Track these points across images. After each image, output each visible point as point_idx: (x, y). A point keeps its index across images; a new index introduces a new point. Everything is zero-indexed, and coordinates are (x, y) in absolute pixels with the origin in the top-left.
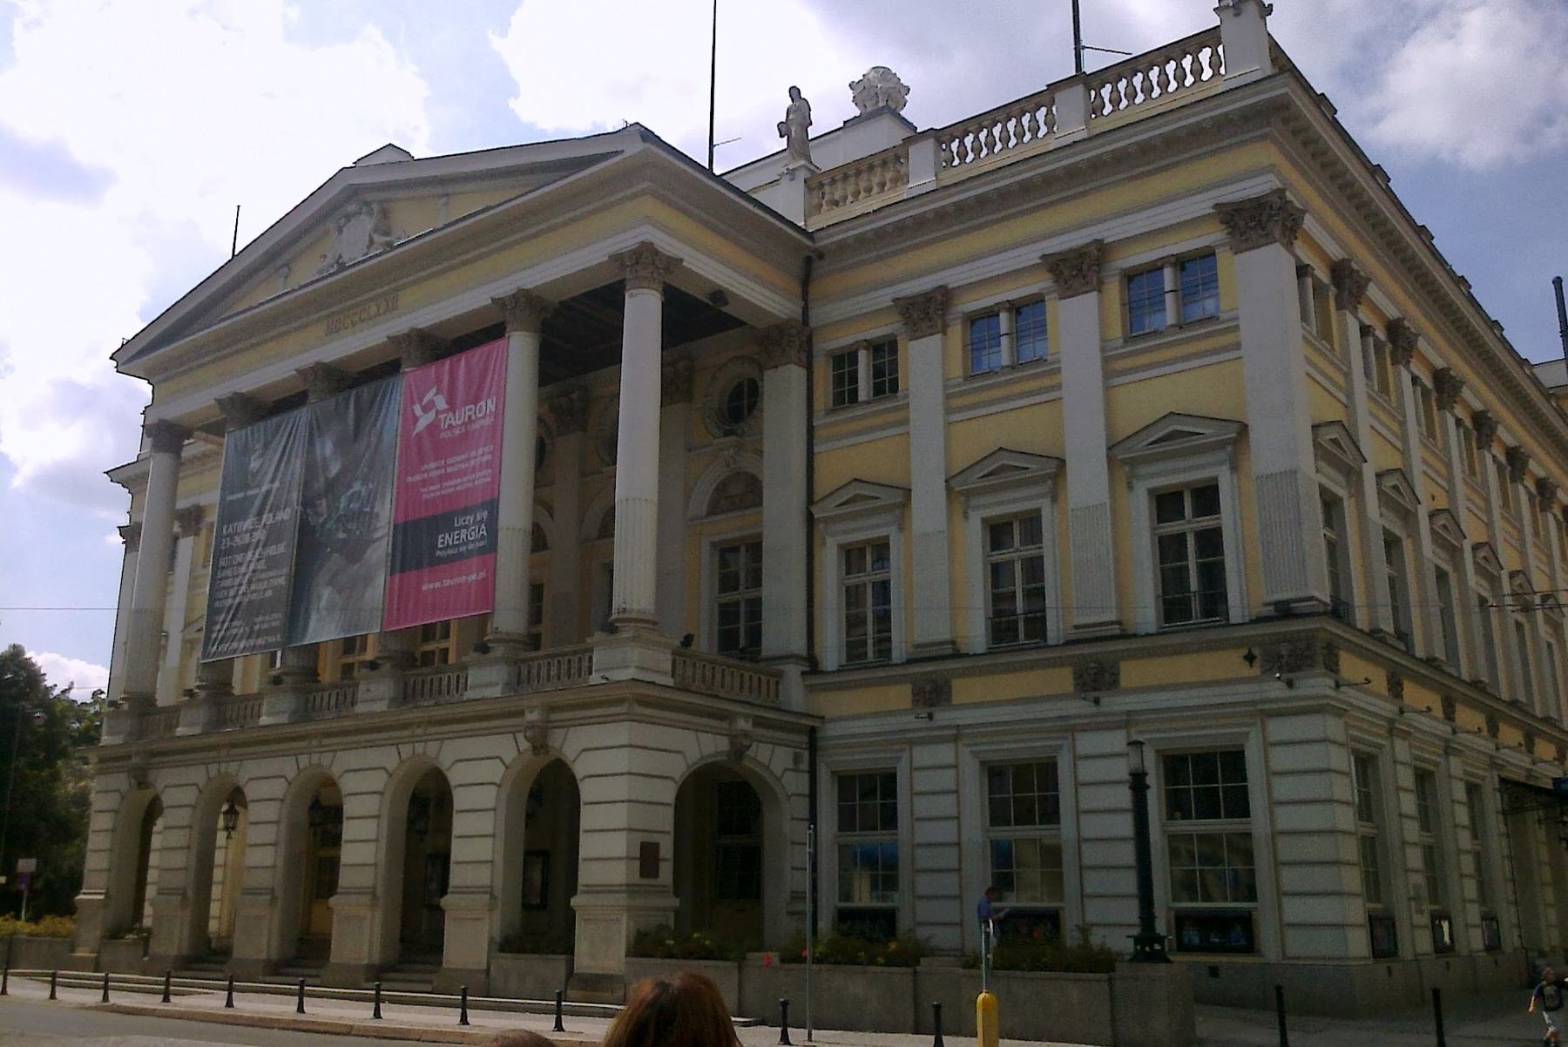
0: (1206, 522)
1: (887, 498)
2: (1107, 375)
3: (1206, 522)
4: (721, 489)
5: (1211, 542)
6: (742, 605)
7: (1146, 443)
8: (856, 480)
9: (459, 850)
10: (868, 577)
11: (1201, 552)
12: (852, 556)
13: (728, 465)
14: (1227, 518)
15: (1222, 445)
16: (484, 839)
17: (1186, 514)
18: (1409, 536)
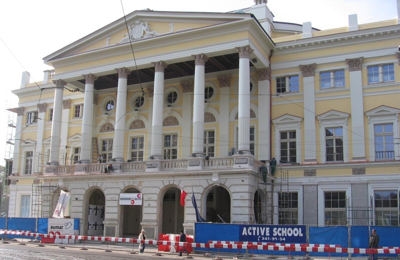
0: (293, 140)
1: (296, 119)
2: (363, 93)
3: (293, 140)
4: (134, 122)
5: (293, 145)
6: (138, 153)
7: (375, 112)
8: (332, 110)
9: (107, 210)
10: (288, 140)
11: (291, 146)
12: (283, 135)
13: (169, 114)
14: (298, 140)
15: (344, 118)
16: (154, 208)
17: (288, 138)
18: (383, 144)
